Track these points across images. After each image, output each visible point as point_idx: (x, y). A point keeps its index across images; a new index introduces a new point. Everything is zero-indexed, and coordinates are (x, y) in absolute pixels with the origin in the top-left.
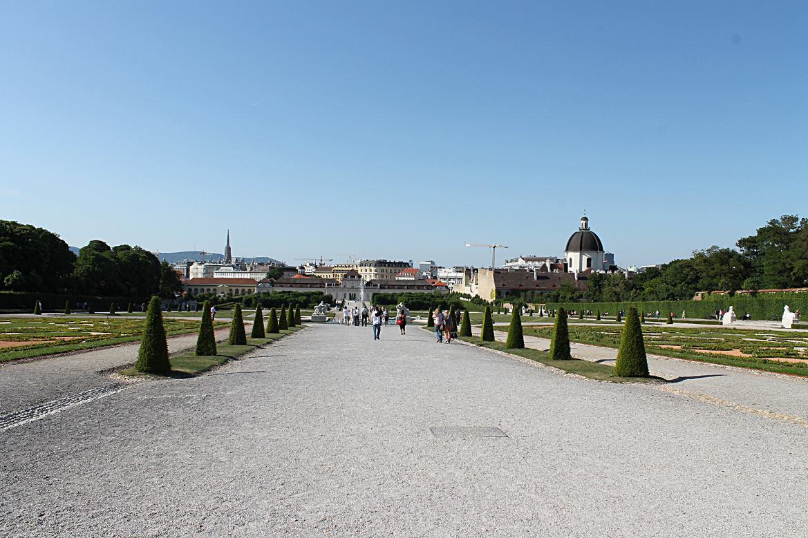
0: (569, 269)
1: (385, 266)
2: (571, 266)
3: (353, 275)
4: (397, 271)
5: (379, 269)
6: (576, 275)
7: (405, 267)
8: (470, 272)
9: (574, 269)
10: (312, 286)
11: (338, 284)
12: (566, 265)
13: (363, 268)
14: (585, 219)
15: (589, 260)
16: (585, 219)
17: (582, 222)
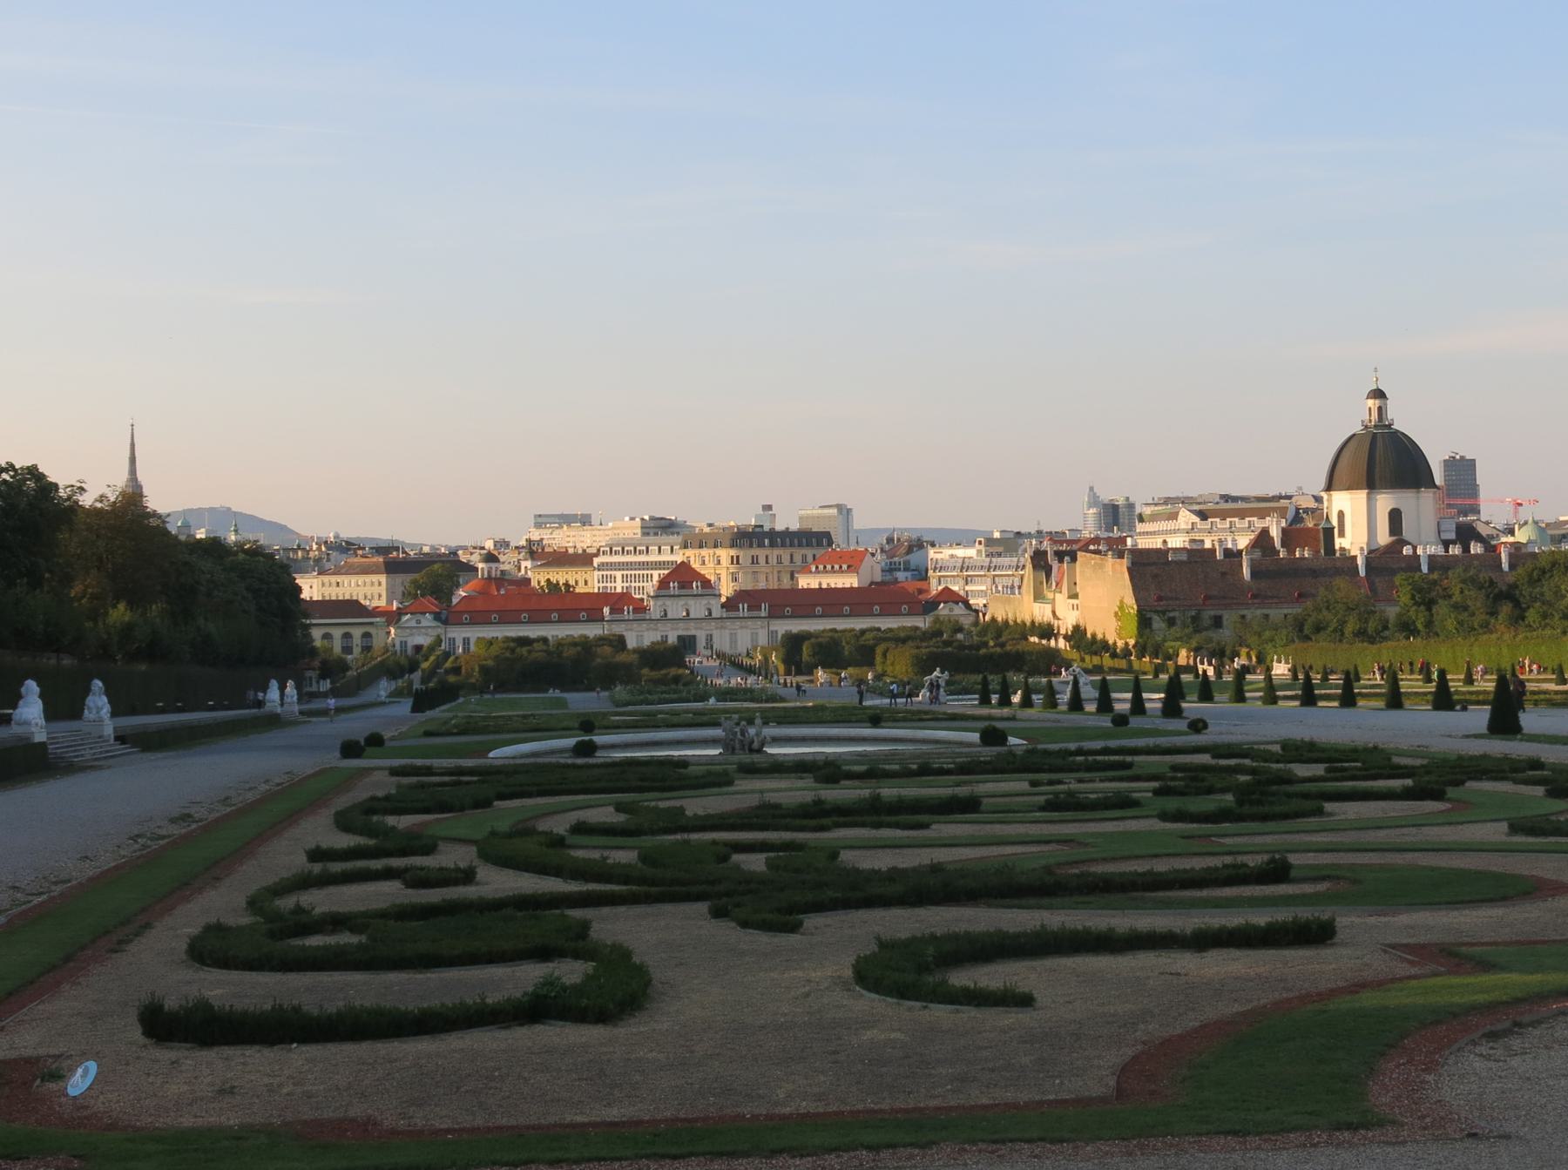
0: (1339, 542)
1: (761, 545)
2: (1342, 534)
3: (682, 578)
4: (798, 558)
5: (745, 555)
6: (1360, 561)
7: (819, 544)
8: (1052, 557)
9: (1353, 541)
10: (568, 616)
11: (640, 608)
12: (1329, 532)
14: (1379, 394)
15: (1395, 517)
16: (1379, 394)
17: (1371, 402)
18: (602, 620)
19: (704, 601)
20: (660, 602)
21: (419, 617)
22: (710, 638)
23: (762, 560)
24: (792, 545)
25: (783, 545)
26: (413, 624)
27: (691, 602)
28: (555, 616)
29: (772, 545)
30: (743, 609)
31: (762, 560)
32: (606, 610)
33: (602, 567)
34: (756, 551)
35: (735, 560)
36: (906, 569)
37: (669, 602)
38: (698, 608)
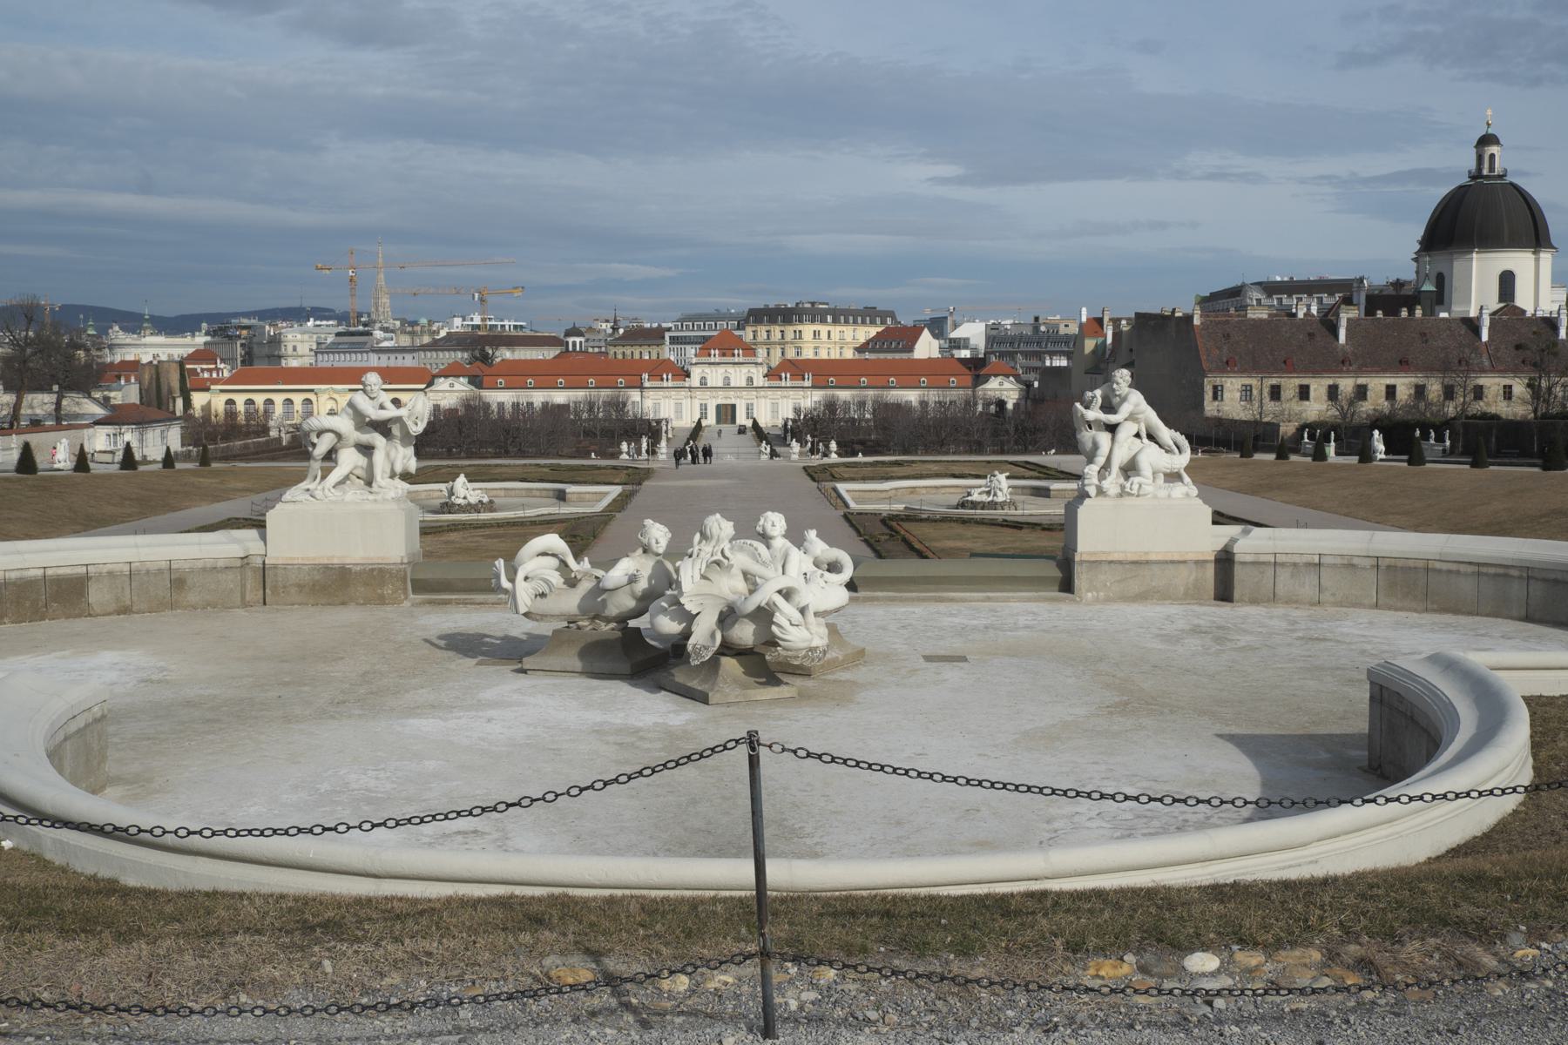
1: (823, 321)
5: (808, 330)
13: (762, 331)
19: (744, 369)
21: (450, 380)
22: (749, 408)
23: (824, 335)
24: (855, 322)
25: (847, 322)
27: (731, 369)
29: (836, 321)
31: (824, 335)
32: (645, 376)
33: (674, 340)
36: (966, 347)
38: (738, 376)
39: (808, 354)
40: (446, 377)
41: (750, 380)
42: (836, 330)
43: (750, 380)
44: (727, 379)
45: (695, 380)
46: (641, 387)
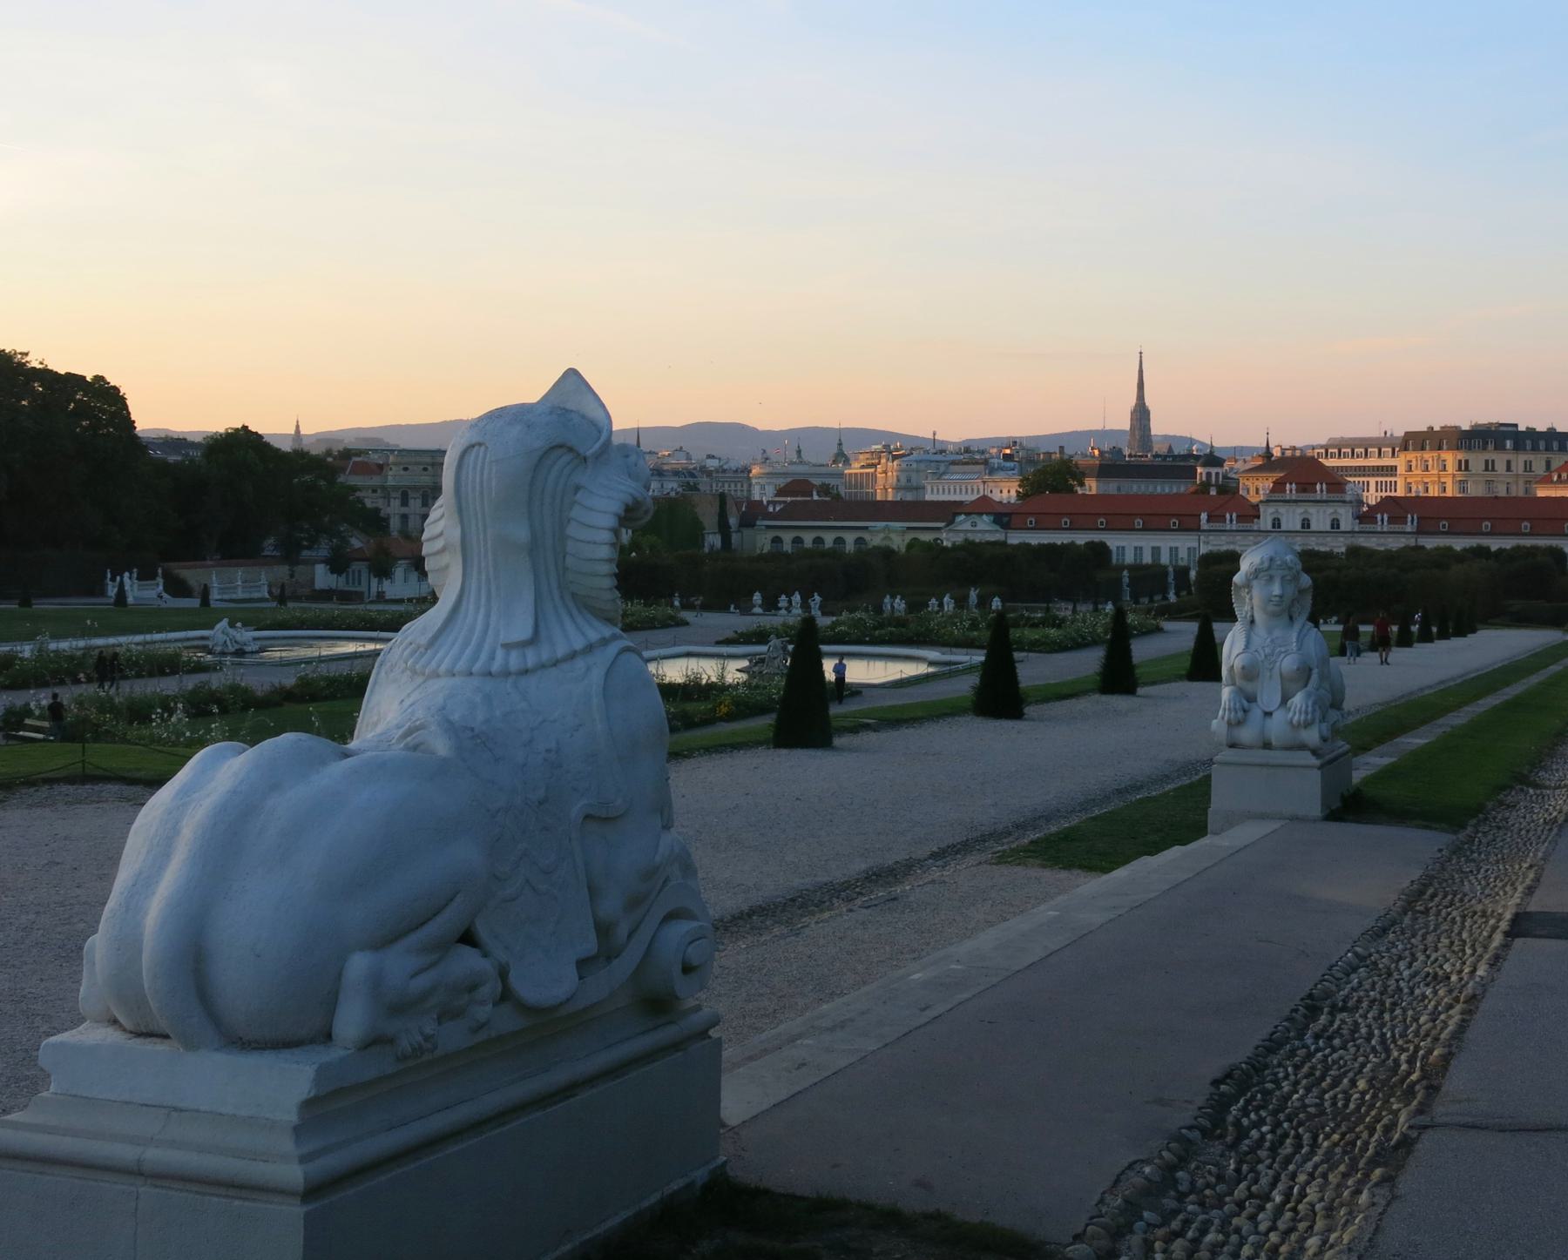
1: (1499, 447)
5: (1477, 460)
18: (1198, 529)
20: (1271, 510)
21: (975, 518)
23: (1500, 467)
24: (1548, 449)
26: (967, 526)
28: (1139, 523)
29: (1518, 447)
30: (1383, 518)
31: (1500, 467)
32: (1204, 516)
34: (1491, 455)
35: (1464, 466)
37: (1282, 509)
39: (1475, 490)
40: (968, 514)
41: (1335, 524)
42: (1519, 460)
43: (1335, 524)
44: (1306, 524)
45: (1265, 522)
46: (1197, 529)
